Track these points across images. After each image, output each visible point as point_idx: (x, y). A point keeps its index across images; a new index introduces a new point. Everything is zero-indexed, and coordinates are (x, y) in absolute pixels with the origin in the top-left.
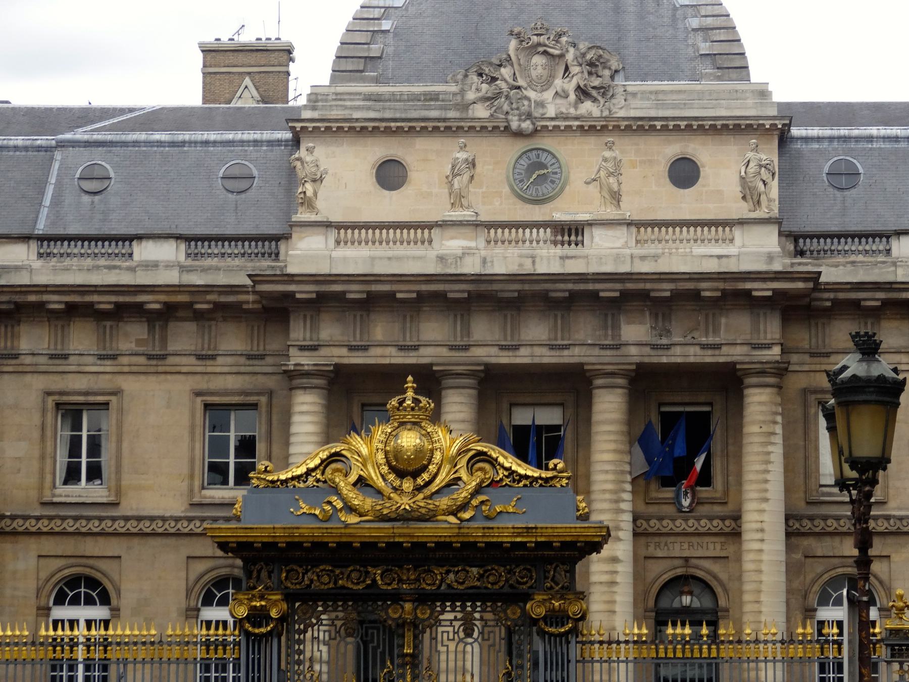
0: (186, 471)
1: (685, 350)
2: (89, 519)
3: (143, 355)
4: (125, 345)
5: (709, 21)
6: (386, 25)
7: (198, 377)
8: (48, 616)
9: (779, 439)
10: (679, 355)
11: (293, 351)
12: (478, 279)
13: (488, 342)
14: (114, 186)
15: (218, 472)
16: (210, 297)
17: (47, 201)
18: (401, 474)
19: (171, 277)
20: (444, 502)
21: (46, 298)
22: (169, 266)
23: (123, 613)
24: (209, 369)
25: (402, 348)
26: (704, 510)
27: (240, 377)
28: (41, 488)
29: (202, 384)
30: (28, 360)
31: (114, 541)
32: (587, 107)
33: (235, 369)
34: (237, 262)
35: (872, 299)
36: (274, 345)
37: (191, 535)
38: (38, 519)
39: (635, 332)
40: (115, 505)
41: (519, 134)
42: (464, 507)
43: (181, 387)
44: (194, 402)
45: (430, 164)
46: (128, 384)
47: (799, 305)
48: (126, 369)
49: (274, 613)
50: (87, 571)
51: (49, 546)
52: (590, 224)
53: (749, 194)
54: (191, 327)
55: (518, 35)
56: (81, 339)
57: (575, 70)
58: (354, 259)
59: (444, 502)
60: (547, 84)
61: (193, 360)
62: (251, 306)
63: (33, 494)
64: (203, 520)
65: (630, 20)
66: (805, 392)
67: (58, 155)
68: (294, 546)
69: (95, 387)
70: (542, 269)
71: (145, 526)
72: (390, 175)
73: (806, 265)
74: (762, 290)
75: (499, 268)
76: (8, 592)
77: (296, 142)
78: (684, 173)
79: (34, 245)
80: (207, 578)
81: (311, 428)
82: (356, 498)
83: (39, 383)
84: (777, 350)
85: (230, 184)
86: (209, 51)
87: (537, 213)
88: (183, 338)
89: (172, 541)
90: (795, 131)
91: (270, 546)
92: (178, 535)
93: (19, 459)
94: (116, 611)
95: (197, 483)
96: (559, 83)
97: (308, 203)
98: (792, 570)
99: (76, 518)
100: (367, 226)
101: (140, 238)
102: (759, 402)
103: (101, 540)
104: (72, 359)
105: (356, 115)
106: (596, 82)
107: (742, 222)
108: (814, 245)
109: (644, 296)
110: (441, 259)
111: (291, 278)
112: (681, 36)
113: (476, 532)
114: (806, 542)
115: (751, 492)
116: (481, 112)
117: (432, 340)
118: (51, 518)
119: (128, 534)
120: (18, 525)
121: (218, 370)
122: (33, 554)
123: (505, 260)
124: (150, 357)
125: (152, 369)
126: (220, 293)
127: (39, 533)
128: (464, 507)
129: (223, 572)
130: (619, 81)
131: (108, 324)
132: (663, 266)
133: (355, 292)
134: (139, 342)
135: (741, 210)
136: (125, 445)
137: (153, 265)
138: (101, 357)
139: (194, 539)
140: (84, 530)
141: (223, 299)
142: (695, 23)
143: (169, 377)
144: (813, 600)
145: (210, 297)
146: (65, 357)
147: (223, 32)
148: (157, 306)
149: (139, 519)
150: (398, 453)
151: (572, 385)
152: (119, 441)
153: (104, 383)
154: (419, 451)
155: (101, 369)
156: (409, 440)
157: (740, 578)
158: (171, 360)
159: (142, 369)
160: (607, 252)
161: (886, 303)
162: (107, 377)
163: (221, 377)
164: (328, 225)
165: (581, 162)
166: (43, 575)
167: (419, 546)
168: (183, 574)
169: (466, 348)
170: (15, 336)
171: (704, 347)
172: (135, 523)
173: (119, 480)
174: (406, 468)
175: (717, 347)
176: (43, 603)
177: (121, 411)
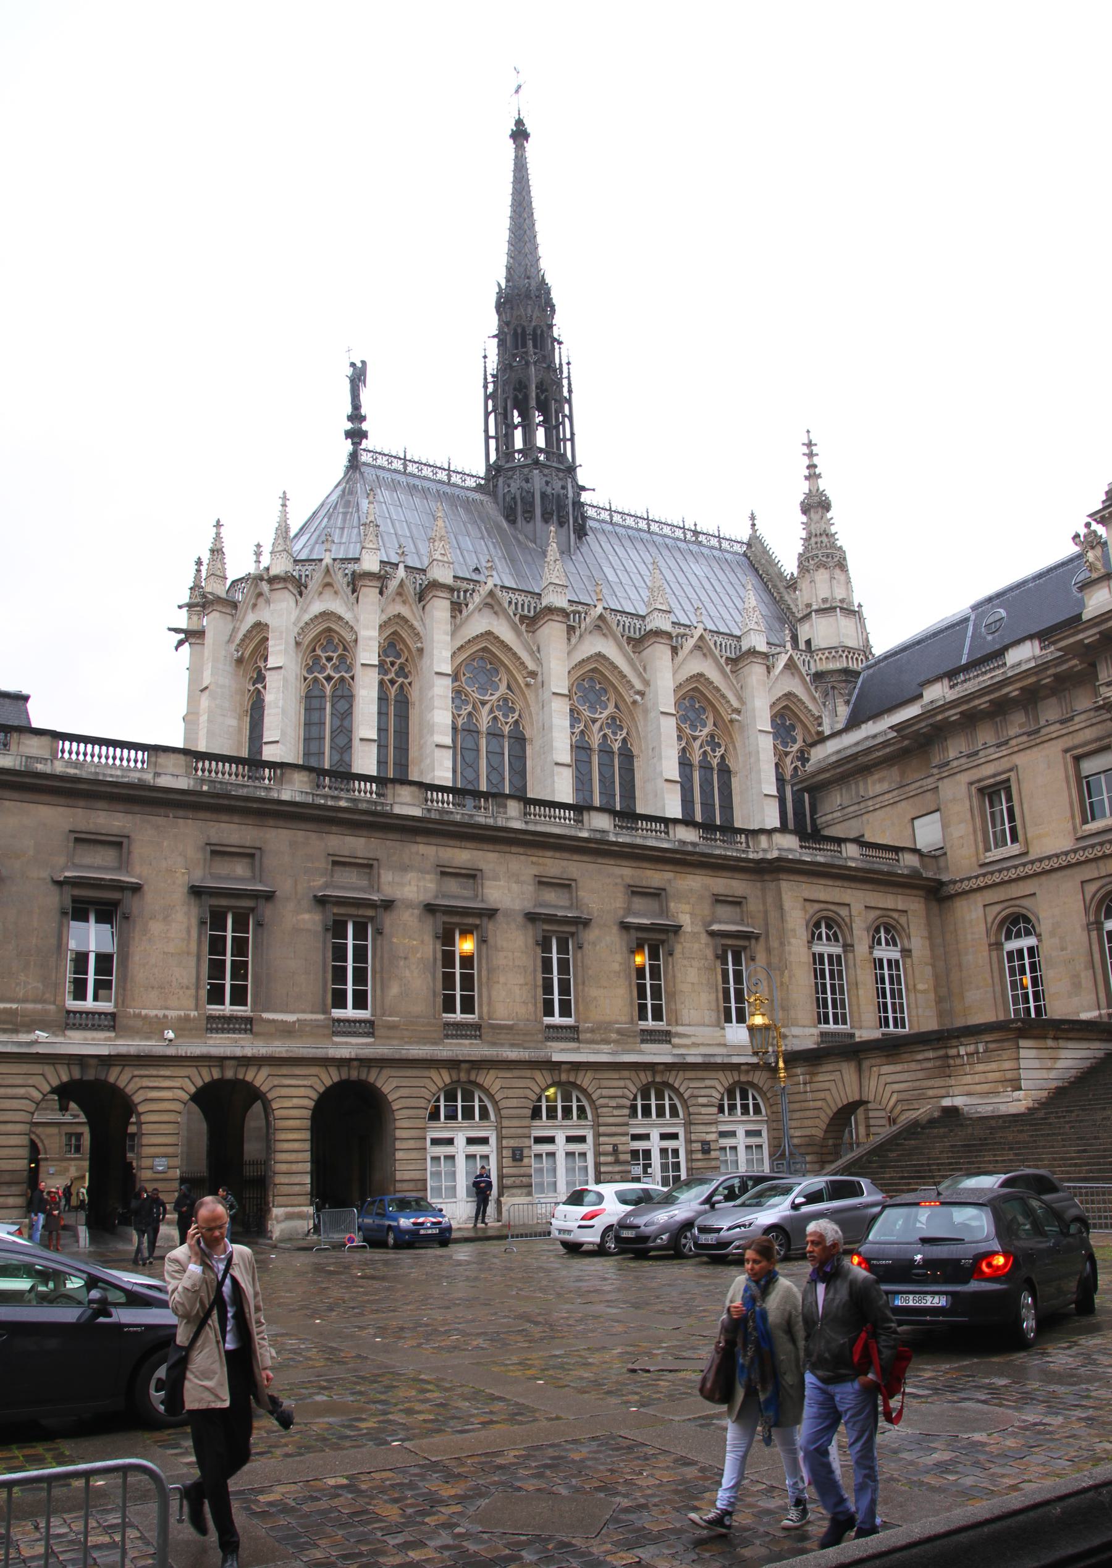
0: (1068, 814)
2: (1008, 869)
3: (1024, 734)
4: (1012, 732)
7: (1066, 738)
8: (1002, 950)
11: (1103, 690)
16: (1049, 672)
21: (947, 714)
22: (1028, 660)
23: (1043, 937)
24: (1071, 729)
27: (1094, 728)
28: (977, 854)
29: (1069, 742)
30: (955, 764)
31: (1029, 881)
33: (1088, 723)
37: (1079, 864)
38: (976, 877)
40: (1026, 853)
43: (1054, 750)
44: (1064, 758)
46: (1019, 760)
48: (1016, 749)
50: (1016, 909)
54: (1053, 701)
56: (985, 736)
61: (1058, 726)
62: (1079, 668)
63: (974, 859)
64: (1084, 849)
69: (1000, 769)
71: (1046, 865)
76: (969, 937)
79: (946, 681)
80: (1099, 896)
83: (964, 778)
88: (1050, 711)
89: (1068, 872)
92: (1070, 866)
93: (961, 837)
95: (1078, 821)
99: (1000, 871)
103: (1021, 883)
104: (981, 753)
118: (984, 875)
119: (1036, 875)
120: (966, 886)
121: (1077, 727)
122: (980, 905)
124: (1029, 734)
125: (1033, 743)
126: (1056, 666)
127: (980, 889)
131: (998, 719)
134: (1021, 726)
136: (1025, 806)
137: (1019, 664)
138: (999, 745)
139: (1084, 866)
140: (1006, 879)
141: (1059, 670)
143: (1046, 745)
145: (1049, 672)
146: (976, 753)
148: (1016, 693)
149: (1040, 860)
152: (1021, 804)
153: (1005, 764)
155: (1000, 754)
158: (1044, 731)
159: (1027, 745)
162: (1006, 759)
163: (1081, 733)
166: (990, 919)
168: (1081, 897)
172: (1038, 864)
173: (1025, 834)
176: (993, 940)
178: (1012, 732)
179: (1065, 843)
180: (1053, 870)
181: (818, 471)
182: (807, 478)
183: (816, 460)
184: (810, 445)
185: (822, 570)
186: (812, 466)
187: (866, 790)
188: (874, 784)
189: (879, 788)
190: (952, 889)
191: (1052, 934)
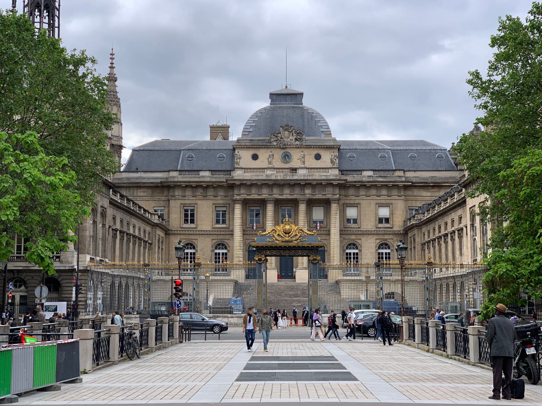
1: (319, 196)
4: (198, 194)
5: (323, 124)
6: (254, 124)
9: (338, 214)
10: (317, 197)
12: (275, 180)
13: (276, 194)
14: (194, 159)
15: (218, 222)
17: (180, 162)
18: (286, 233)
19: (208, 179)
20: (294, 239)
22: (208, 177)
25: (258, 195)
26: (322, 229)
28: (180, 224)
29: (215, 202)
30: (177, 197)
32: (297, 142)
34: (222, 176)
35: (358, 184)
36: (230, 194)
39: (308, 191)
41: (283, 148)
42: (297, 240)
45: (264, 155)
46: (199, 202)
47: (343, 186)
49: (263, 259)
51: (182, 237)
52: (298, 168)
53: (332, 162)
54: (212, 190)
55: (282, 127)
56: (188, 192)
57: (295, 135)
58: (248, 176)
59: (294, 239)
60: (289, 137)
63: (179, 225)
65: (306, 124)
66: (344, 204)
67: (182, 152)
68: (266, 247)
70: (288, 178)
71: (203, 233)
72: (255, 157)
73: (344, 177)
74: (335, 183)
75: (279, 178)
77: (234, 149)
78: (318, 157)
79: (178, 172)
81: (240, 212)
82: (278, 238)
84: (338, 195)
85: (219, 159)
86: (211, 127)
87: (287, 166)
88: (211, 192)
90: (341, 148)
91: (263, 247)
94: (197, 251)
96: (291, 137)
97: (238, 164)
98: (341, 242)
100: (251, 169)
101: (201, 171)
102: (334, 207)
105: (248, 144)
106: (299, 137)
107: (330, 168)
108: (345, 173)
109: (310, 184)
110: (267, 175)
111: (235, 180)
112: (317, 127)
113: (300, 244)
114: (343, 236)
115: (332, 225)
116: (275, 143)
117: (265, 194)
123: (280, 176)
128: (297, 240)
129: (219, 242)
130: (304, 136)
132: (314, 178)
133: (249, 183)
134: (201, 193)
135: (330, 165)
142: (319, 124)
144: (345, 248)
147: (214, 123)
149: (202, 231)
150: (285, 229)
151: (295, 203)
152: (197, 215)
154: (289, 229)
156: (287, 227)
157: (330, 243)
160: (302, 174)
161: (361, 185)
164: (242, 168)
165: (296, 156)
167: (290, 247)
169: (272, 195)
170: (174, 192)
171: (323, 195)
174: (287, 233)
175: (325, 195)
177: (197, 208)
178: (198, 194)
179: (209, 228)
180: (205, 234)
181: (114, 65)
182: (110, 67)
183: (114, 61)
184: (112, 54)
185: (115, 106)
186: (112, 63)
187: (137, 193)
188: (140, 192)
189: (142, 194)
190: (171, 232)
191: (201, 251)
